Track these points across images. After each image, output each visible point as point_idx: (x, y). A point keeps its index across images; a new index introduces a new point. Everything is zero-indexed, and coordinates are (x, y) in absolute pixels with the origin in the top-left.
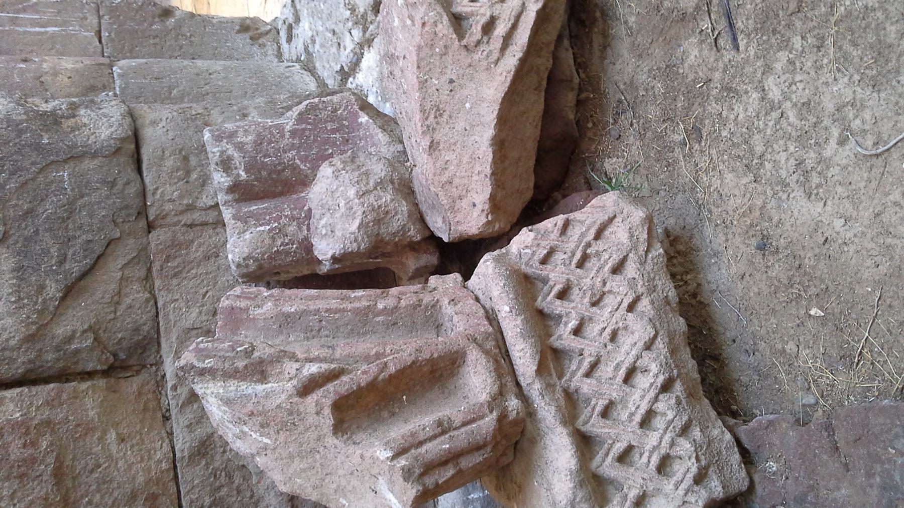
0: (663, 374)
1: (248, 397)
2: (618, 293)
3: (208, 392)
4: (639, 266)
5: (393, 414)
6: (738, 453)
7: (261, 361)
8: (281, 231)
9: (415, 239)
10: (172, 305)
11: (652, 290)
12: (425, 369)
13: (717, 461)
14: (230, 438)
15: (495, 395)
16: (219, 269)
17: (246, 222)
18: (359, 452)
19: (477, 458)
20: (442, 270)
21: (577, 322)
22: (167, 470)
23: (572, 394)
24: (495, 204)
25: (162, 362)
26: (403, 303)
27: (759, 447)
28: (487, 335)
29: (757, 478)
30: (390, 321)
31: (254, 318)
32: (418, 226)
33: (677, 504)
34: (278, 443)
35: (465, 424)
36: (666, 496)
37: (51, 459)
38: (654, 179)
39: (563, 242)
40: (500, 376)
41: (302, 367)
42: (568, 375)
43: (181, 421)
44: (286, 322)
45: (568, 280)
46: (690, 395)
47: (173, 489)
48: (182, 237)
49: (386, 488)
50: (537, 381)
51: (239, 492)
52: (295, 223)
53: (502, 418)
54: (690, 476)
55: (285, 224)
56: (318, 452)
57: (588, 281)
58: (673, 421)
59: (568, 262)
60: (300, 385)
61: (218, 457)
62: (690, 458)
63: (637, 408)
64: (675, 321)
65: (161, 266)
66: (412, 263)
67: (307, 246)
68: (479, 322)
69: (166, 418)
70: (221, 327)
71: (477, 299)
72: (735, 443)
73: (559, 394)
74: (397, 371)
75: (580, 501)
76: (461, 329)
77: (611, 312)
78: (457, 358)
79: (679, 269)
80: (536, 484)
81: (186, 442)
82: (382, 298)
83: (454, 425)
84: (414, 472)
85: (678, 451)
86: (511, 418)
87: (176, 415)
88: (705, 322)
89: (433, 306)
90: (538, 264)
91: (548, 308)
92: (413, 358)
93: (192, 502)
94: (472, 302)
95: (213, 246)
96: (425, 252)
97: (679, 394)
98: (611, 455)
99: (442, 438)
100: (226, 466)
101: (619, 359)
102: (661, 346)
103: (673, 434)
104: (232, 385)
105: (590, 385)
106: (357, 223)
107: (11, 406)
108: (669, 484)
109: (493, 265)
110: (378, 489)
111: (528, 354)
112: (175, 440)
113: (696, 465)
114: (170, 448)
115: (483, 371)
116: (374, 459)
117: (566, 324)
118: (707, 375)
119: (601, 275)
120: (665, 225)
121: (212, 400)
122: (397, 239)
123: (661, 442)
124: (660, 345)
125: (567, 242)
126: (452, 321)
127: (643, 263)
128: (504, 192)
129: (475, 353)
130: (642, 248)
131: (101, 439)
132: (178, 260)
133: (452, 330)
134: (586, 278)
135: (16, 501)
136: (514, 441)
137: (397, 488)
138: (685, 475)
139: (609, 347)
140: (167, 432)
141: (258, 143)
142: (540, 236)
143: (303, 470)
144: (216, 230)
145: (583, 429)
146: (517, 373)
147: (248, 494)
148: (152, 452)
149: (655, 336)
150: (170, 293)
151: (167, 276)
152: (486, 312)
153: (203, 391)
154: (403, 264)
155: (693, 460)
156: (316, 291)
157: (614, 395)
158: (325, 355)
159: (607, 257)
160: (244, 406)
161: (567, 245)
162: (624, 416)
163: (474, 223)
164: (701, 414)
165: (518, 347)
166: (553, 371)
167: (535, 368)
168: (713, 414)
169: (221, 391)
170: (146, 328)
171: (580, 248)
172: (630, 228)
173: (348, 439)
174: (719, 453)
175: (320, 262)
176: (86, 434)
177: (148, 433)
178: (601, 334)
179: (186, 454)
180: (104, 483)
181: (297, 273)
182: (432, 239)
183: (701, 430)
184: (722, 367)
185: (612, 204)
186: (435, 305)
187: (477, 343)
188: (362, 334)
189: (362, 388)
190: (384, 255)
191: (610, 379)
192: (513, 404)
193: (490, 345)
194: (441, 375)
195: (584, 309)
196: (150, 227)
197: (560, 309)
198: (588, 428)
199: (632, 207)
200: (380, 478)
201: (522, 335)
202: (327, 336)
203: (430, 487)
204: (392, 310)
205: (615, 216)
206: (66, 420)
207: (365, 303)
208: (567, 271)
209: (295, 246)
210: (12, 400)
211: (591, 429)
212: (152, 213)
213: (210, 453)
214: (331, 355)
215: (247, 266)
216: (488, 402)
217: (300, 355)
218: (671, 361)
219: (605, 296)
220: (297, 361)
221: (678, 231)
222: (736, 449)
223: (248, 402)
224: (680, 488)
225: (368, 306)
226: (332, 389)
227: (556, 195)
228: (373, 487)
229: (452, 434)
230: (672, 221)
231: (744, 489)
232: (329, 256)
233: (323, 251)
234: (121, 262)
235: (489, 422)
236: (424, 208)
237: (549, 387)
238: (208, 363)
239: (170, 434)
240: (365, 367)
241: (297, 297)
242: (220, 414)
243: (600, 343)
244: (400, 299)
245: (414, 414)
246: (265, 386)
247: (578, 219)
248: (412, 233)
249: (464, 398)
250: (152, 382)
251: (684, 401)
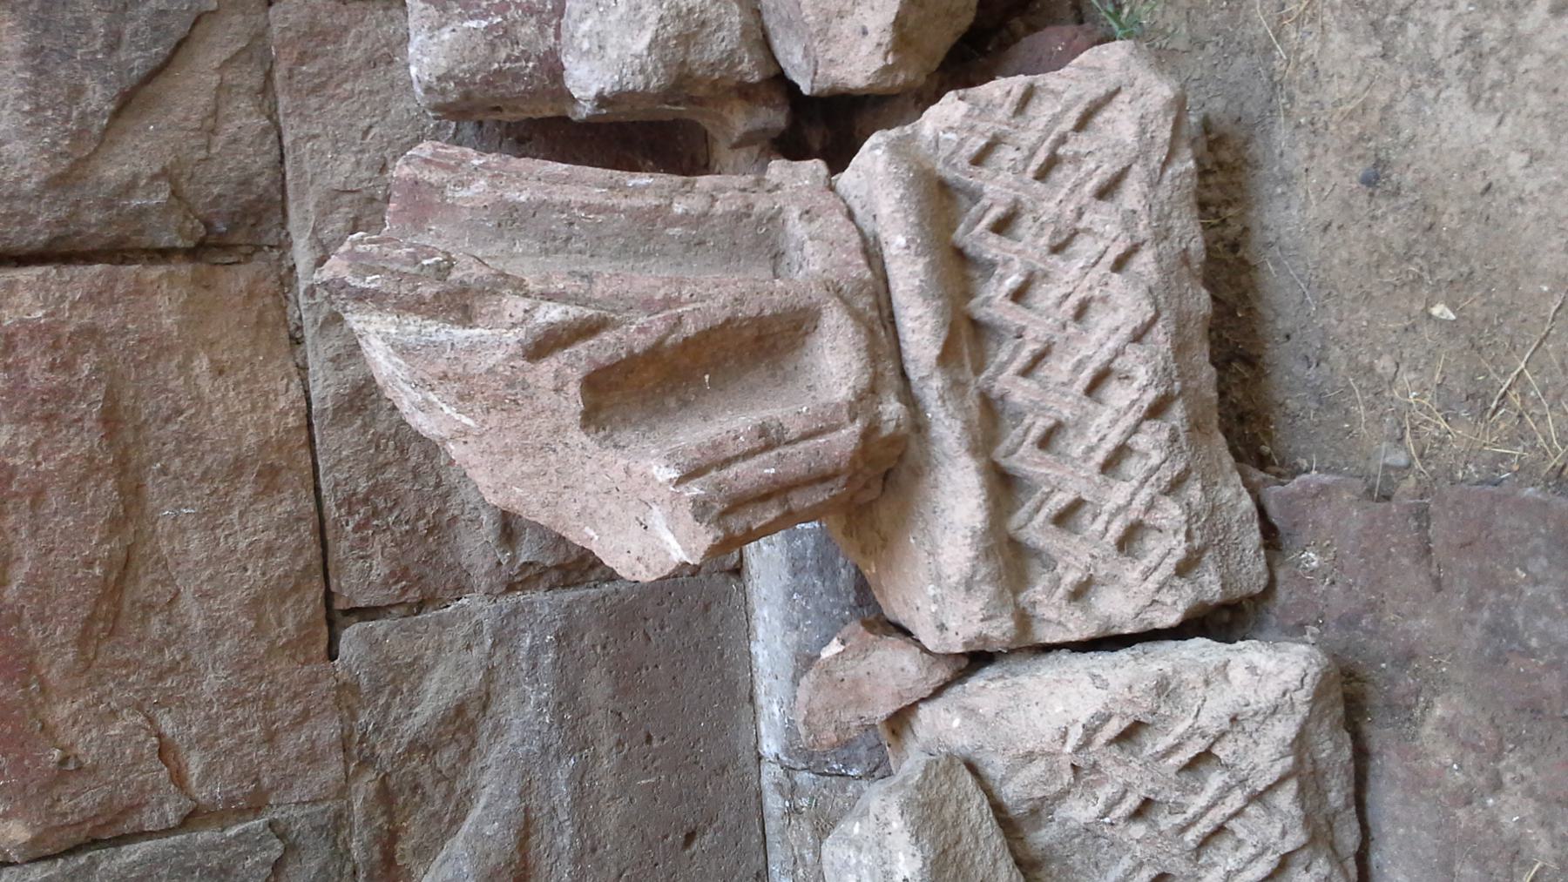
0: (1156, 387)
1: (438, 347)
2: (1102, 235)
3: (371, 329)
4: (1146, 189)
5: (685, 404)
6: (1258, 532)
7: (464, 290)
8: (507, 33)
9: (748, 79)
10: (309, 145)
11: (1162, 235)
12: (747, 333)
13: (1220, 541)
14: (405, 407)
15: (863, 390)
16: (392, 86)
17: (445, 9)
18: (622, 462)
19: (820, 495)
20: (791, 147)
21: (1022, 279)
22: (298, 429)
23: (995, 401)
24: (903, 35)
25: (291, 244)
26: (719, 208)
27: (1295, 525)
28: (861, 285)
29: (1281, 574)
30: (694, 237)
31: (453, 205)
32: (760, 55)
33: (1141, 604)
34: (487, 427)
35: (806, 436)
36: (1126, 588)
37: (97, 394)
38: (1201, 19)
39: (1017, 127)
40: (874, 358)
41: (535, 307)
42: (992, 369)
43: (321, 348)
44: (510, 218)
45: (1017, 201)
46: (1196, 426)
48: (328, 21)
49: (664, 524)
50: (937, 374)
51: (416, 476)
52: (533, 21)
53: (869, 433)
54: (1171, 561)
55: (516, 21)
56: (555, 451)
57: (1051, 207)
58: (1158, 468)
59: (1020, 167)
60: (530, 341)
61: (383, 415)
62: (1176, 533)
63: (1101, 440)
64: (1193, 296)
65: (290, 70)
66: (740, 121)
67: (554, 69)
68: (849, 259)
69: (296, 341)
70: (395, 214)
71: (851, 215)
72: (1256, 516)
73: (972, 401)
74: (698, 334)
75: (981, 581)
76: (817, 268)
77: (1082, 268)
78: (803, 321)
79: (1214, 195)
80: (912, 541)
81: (329, 386)
82: (682, 195)
83: (787, 437)
84: (713, 507)
85: (1157, 518)
86: (885, 433)
87: (313, 337)
88: (1243, 297)
89: (771, 219)
90: (966, 163)
91: (974, 246)
92: (728, 312)
93: (337, 485)
94: (841, 219)
95: (383, 42)
96: (766, 103)
97: (1175, 423)
98: (1044, 511)
99: (765, 456)
100: (397, 433)
101: (1084, 353)
102: (1161, 338)
103: (1155, 490)
104: (413, 323)
105: (1026, 390)
106: (647, 37)
107: (28, 298)
108: (1134, 569)
109: (885, 157)
110: (649, 523)
111: (928, 327)
112: (310, 380)
113: (1184, 545)
114: (301, 393)
115: (846, 348)
116: (648, 479)
117: (1002, 278)
118: (1229, 388)
119: (1076, 198)
120: (1204, 110)
121: (377, 343)
122: (717, 76)
123: (1132, 500)
124: (1160, 337)
125: (1025, 129)
126: (802, 250)
127: (1155, 183)
128: (923, 13)
129: (835, 315)
130: (1158, 156)
131: (184, 367)
132: (320, 63)
133: (801, 267)
134: (1049, 200)
135: (40, 458)
136: (884, 469)
137: (682, 528)
138: (1163, 558)
139: (1071, 330)
140: (297, 366)
142: (977, 112)
143: (529, 476)
144: (390, 13)
145: (1004, 463)
146: (904, 356)
148: (272, 396)
149: (1154, 321)
150: (304, 121)
151: (299, 91)
152: (864, 240)
153: (361, 325)
154: (724, 121)
155: (1181, 537)
156: (566, 166)
157: (1066, 412)
158: (575, 289)
159: (1093, 166)
160: (432, 363)
161: (1023, 135)
162: (1077, 450)
163: (859, 66)
164: (1207, 461)
165: (913, 312)
166: (967, 360)
167: (937, 352)
168: (1228, 461)
169: (393, 330)
170: (263, 181)
171: (1047, 144)
172: (1142, 117)
173: (605, 438)
174: (1227, 529)
175: (574, 101)
176: (157, 357)
177: (265, 363)
178: (1059, 304)
179: (329, 404)
180: (189, 441)
181: (533, 111)
182: (780, 82)
183: (1203, 488)
184: (1258, 379)
185: (1116, 66)
186: (775, 218)
187: (841, 298)
188: (643, 254)
189: (637, 356)
190: (691, 100)
191: (1064, 384)
192: (892, 409)
193: (863, 302)
194: (774, 346)
195: (1037, 256)
197: (994, 251)
198: (1012, 463)
199: (1153, 76)
200: (655, 507)
201: (922, 292)
202: (580, 252)
203: (737, 533)
204: (698, 218)
205: (1118, 91)
206: (122, 331)
207: (652, 201)
208: (1017, 184)
209: (531, 64)
210: (29, 286)
211: (1018, 464)
213: (370, 407)
214: (586, 292)
215: (443, 92)
216: (850, 402)
217: (532, 286)
218: (1174, 366)
219: (1077, 237)
220: (526, 295)
221: (1226, 126)
222: (1256, 525)
223: (440, 357)
224: (1151, 578)
225: (657, 206)
226: (584, 353)
227: (1017, 23)
228: (641, 519)
229: (782, 451)
230: (1218, 104)
231: (1258, 590)
232: (592, 93)
233: (581, 83)
234: (219, 56)
235: (847, 437)
236: (771, 22)
237: (956, 386)
238: (371, 282)
239: (303, 369)
240: (642, 320)
241: (531, 174)
242: (391, 367)
243: (1056, 320)
244: (714, 199)
245: (720, 408)
246: (468, 332)
247: (1051, 87)
248: (745, 66)
249: (810, 388)
250: (273, 277)
251: (1183, 438)
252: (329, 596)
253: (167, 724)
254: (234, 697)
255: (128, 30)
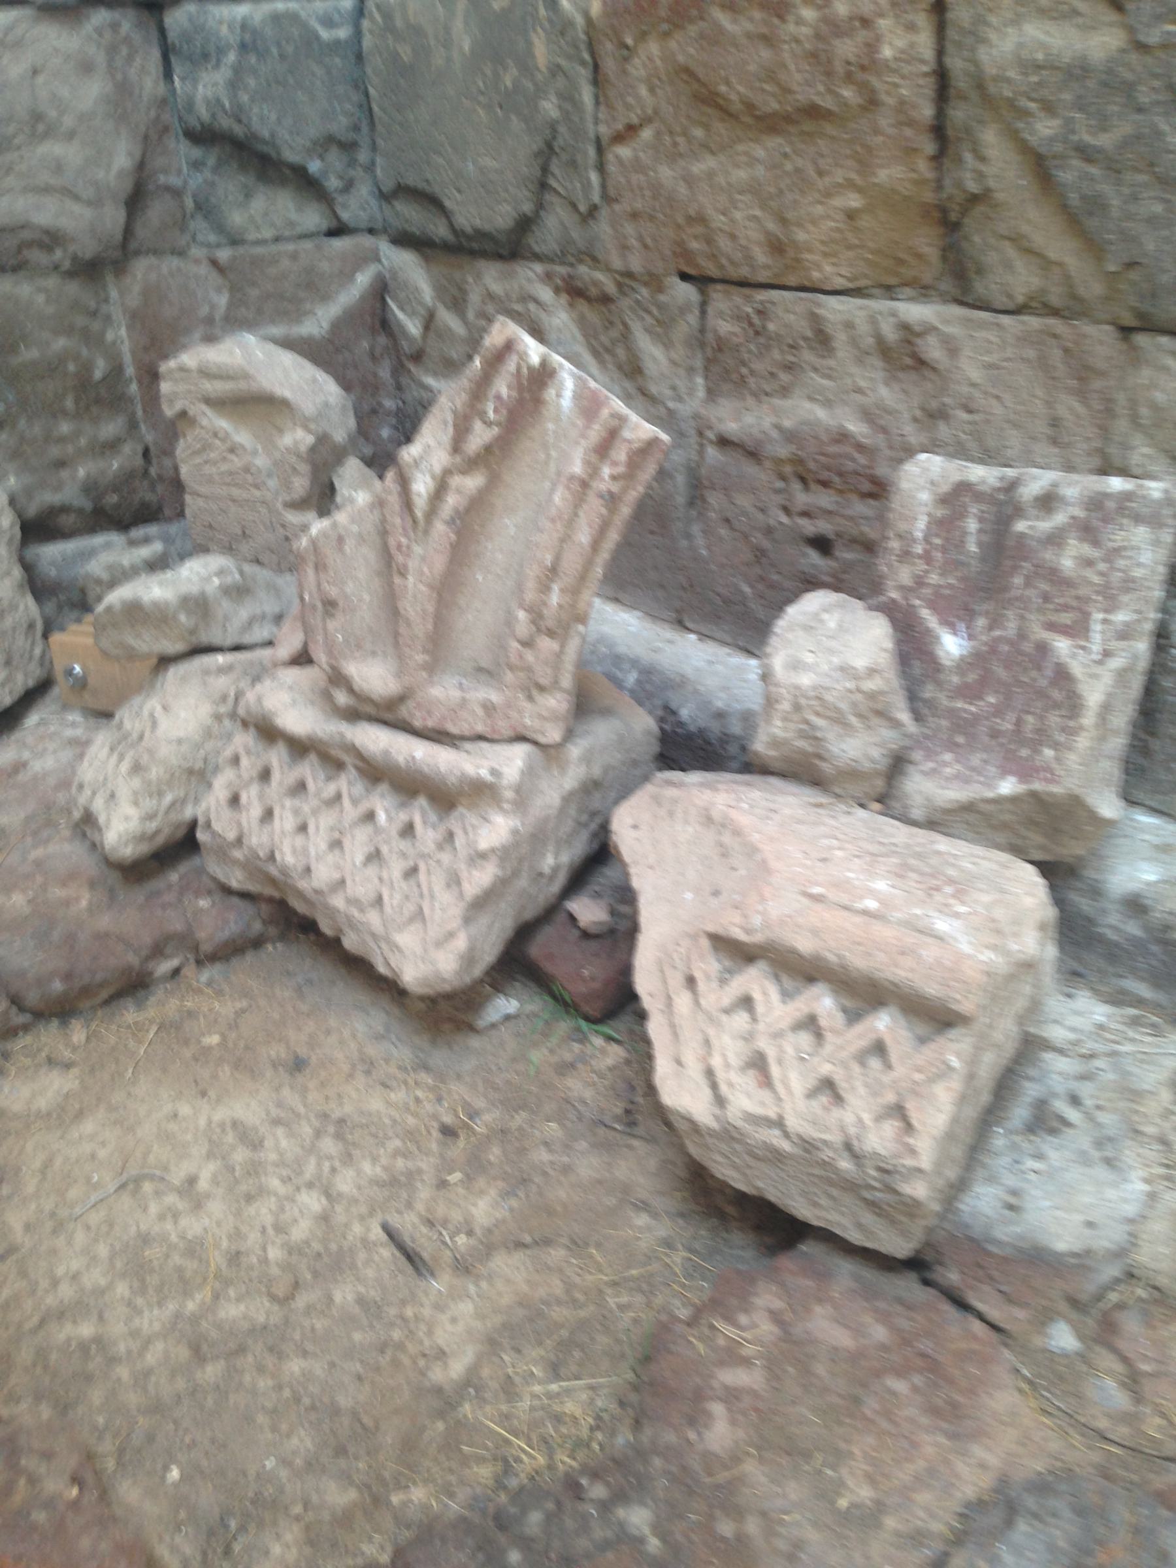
8: (906, 555)
37: (827, 103)
43: (862, 313)
47: (792, 280)
107: (900, 43)
114: (838, 288)
131: (851, 185)
141: (1054, 575)
147: (767, 388)
148: (834, 260)
196: (1126, 331)
206: (877, 131)
212: (1141, 339)
234: (1072, 263)
252: (712, 280)
253: (647, 134)
254: (656, 189)
255: (1094, 170)
